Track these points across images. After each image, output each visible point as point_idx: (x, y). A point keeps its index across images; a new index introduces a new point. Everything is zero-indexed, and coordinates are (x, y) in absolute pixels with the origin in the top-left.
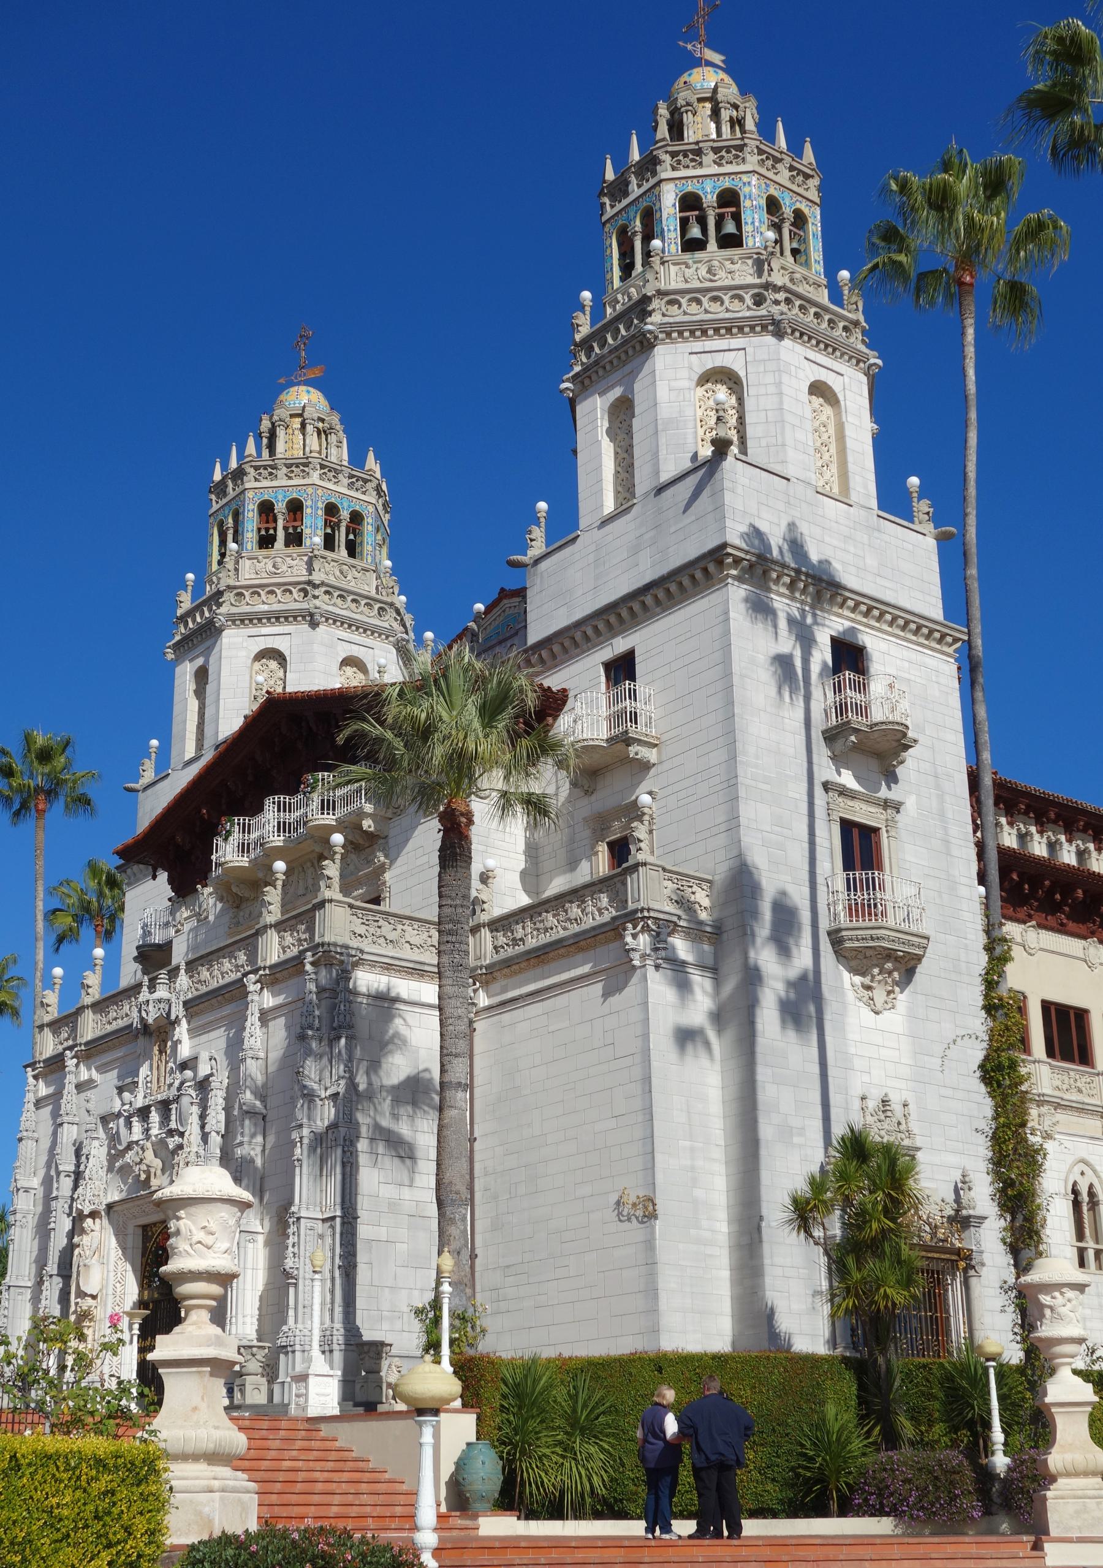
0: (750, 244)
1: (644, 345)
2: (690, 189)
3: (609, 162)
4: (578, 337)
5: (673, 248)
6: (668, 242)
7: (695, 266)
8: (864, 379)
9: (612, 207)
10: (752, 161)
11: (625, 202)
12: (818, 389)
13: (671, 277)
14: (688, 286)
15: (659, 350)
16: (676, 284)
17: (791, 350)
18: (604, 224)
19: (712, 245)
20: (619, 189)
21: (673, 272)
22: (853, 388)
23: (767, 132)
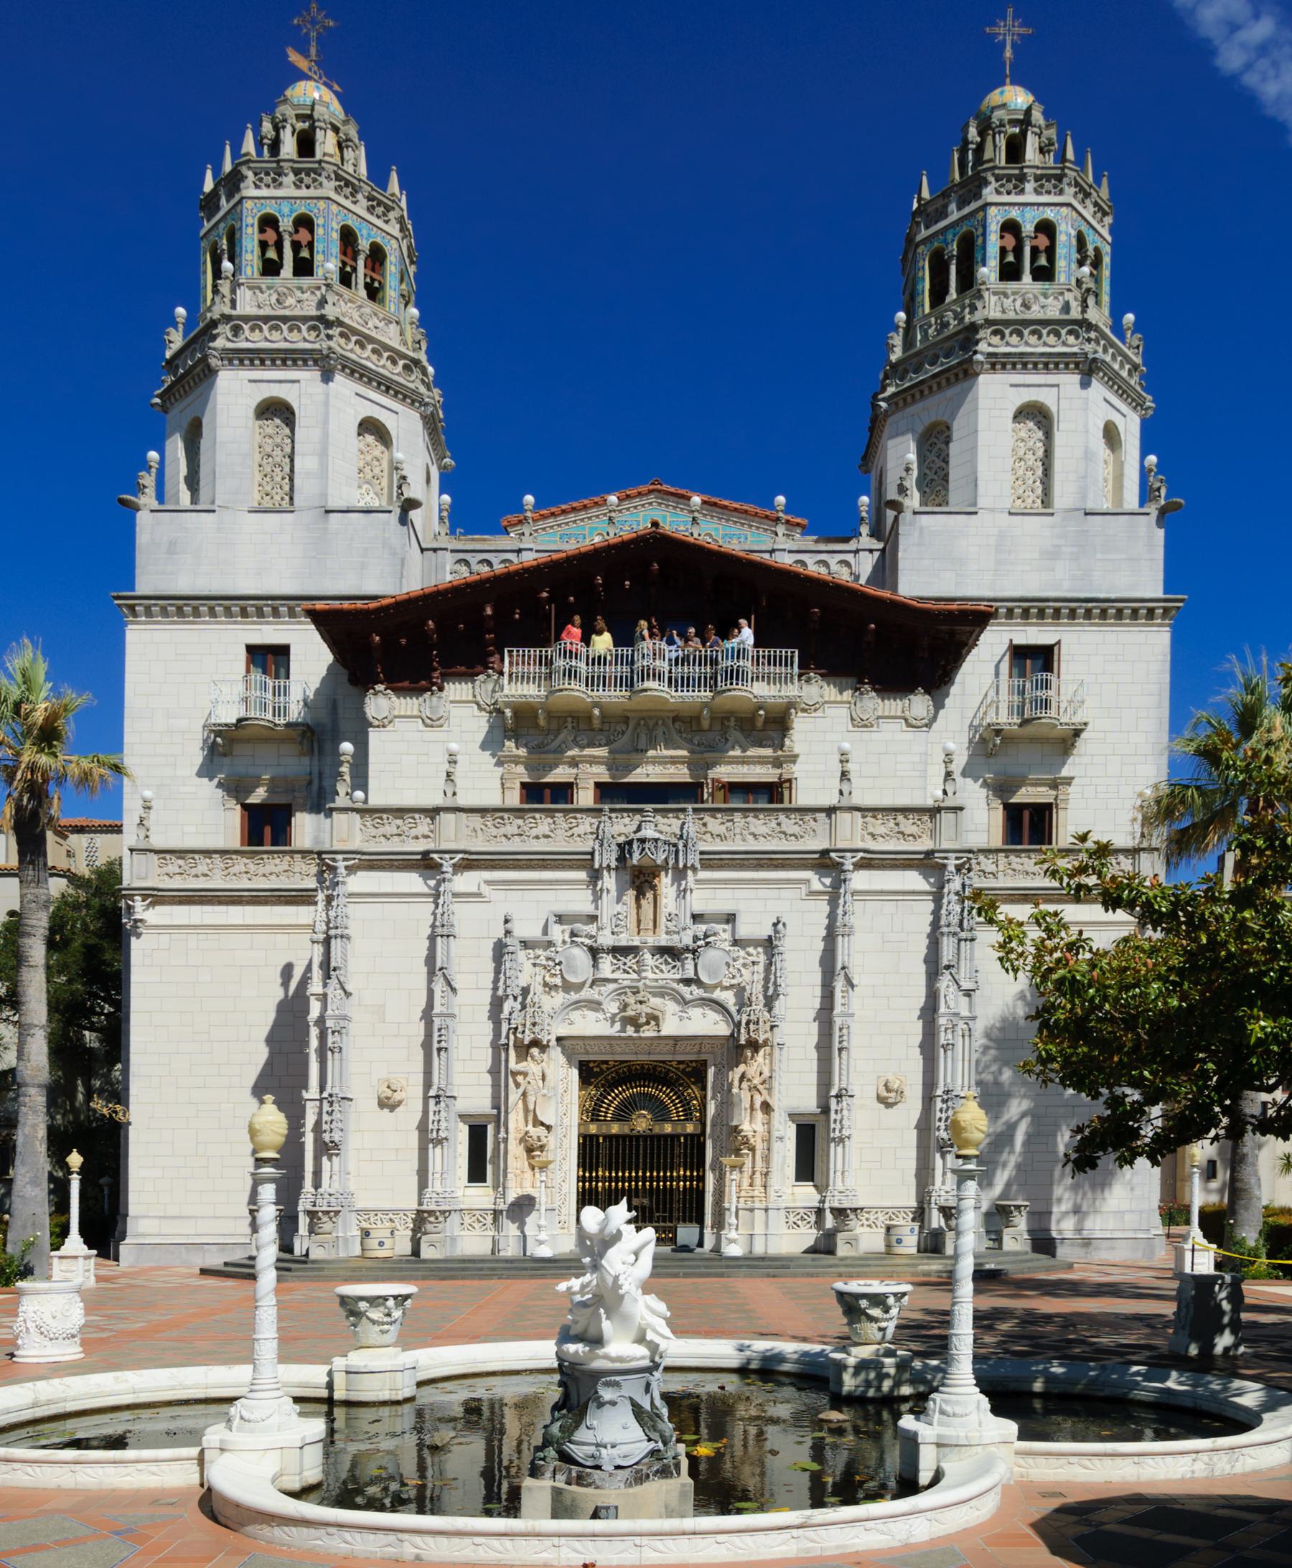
1: (965, 373)
6: (988, 272)
10: (1069, 195)
13: (991, 307)
14: (1005, 317)
16: (995, 314)
19: (1027, 277)
23: (1080, 161)
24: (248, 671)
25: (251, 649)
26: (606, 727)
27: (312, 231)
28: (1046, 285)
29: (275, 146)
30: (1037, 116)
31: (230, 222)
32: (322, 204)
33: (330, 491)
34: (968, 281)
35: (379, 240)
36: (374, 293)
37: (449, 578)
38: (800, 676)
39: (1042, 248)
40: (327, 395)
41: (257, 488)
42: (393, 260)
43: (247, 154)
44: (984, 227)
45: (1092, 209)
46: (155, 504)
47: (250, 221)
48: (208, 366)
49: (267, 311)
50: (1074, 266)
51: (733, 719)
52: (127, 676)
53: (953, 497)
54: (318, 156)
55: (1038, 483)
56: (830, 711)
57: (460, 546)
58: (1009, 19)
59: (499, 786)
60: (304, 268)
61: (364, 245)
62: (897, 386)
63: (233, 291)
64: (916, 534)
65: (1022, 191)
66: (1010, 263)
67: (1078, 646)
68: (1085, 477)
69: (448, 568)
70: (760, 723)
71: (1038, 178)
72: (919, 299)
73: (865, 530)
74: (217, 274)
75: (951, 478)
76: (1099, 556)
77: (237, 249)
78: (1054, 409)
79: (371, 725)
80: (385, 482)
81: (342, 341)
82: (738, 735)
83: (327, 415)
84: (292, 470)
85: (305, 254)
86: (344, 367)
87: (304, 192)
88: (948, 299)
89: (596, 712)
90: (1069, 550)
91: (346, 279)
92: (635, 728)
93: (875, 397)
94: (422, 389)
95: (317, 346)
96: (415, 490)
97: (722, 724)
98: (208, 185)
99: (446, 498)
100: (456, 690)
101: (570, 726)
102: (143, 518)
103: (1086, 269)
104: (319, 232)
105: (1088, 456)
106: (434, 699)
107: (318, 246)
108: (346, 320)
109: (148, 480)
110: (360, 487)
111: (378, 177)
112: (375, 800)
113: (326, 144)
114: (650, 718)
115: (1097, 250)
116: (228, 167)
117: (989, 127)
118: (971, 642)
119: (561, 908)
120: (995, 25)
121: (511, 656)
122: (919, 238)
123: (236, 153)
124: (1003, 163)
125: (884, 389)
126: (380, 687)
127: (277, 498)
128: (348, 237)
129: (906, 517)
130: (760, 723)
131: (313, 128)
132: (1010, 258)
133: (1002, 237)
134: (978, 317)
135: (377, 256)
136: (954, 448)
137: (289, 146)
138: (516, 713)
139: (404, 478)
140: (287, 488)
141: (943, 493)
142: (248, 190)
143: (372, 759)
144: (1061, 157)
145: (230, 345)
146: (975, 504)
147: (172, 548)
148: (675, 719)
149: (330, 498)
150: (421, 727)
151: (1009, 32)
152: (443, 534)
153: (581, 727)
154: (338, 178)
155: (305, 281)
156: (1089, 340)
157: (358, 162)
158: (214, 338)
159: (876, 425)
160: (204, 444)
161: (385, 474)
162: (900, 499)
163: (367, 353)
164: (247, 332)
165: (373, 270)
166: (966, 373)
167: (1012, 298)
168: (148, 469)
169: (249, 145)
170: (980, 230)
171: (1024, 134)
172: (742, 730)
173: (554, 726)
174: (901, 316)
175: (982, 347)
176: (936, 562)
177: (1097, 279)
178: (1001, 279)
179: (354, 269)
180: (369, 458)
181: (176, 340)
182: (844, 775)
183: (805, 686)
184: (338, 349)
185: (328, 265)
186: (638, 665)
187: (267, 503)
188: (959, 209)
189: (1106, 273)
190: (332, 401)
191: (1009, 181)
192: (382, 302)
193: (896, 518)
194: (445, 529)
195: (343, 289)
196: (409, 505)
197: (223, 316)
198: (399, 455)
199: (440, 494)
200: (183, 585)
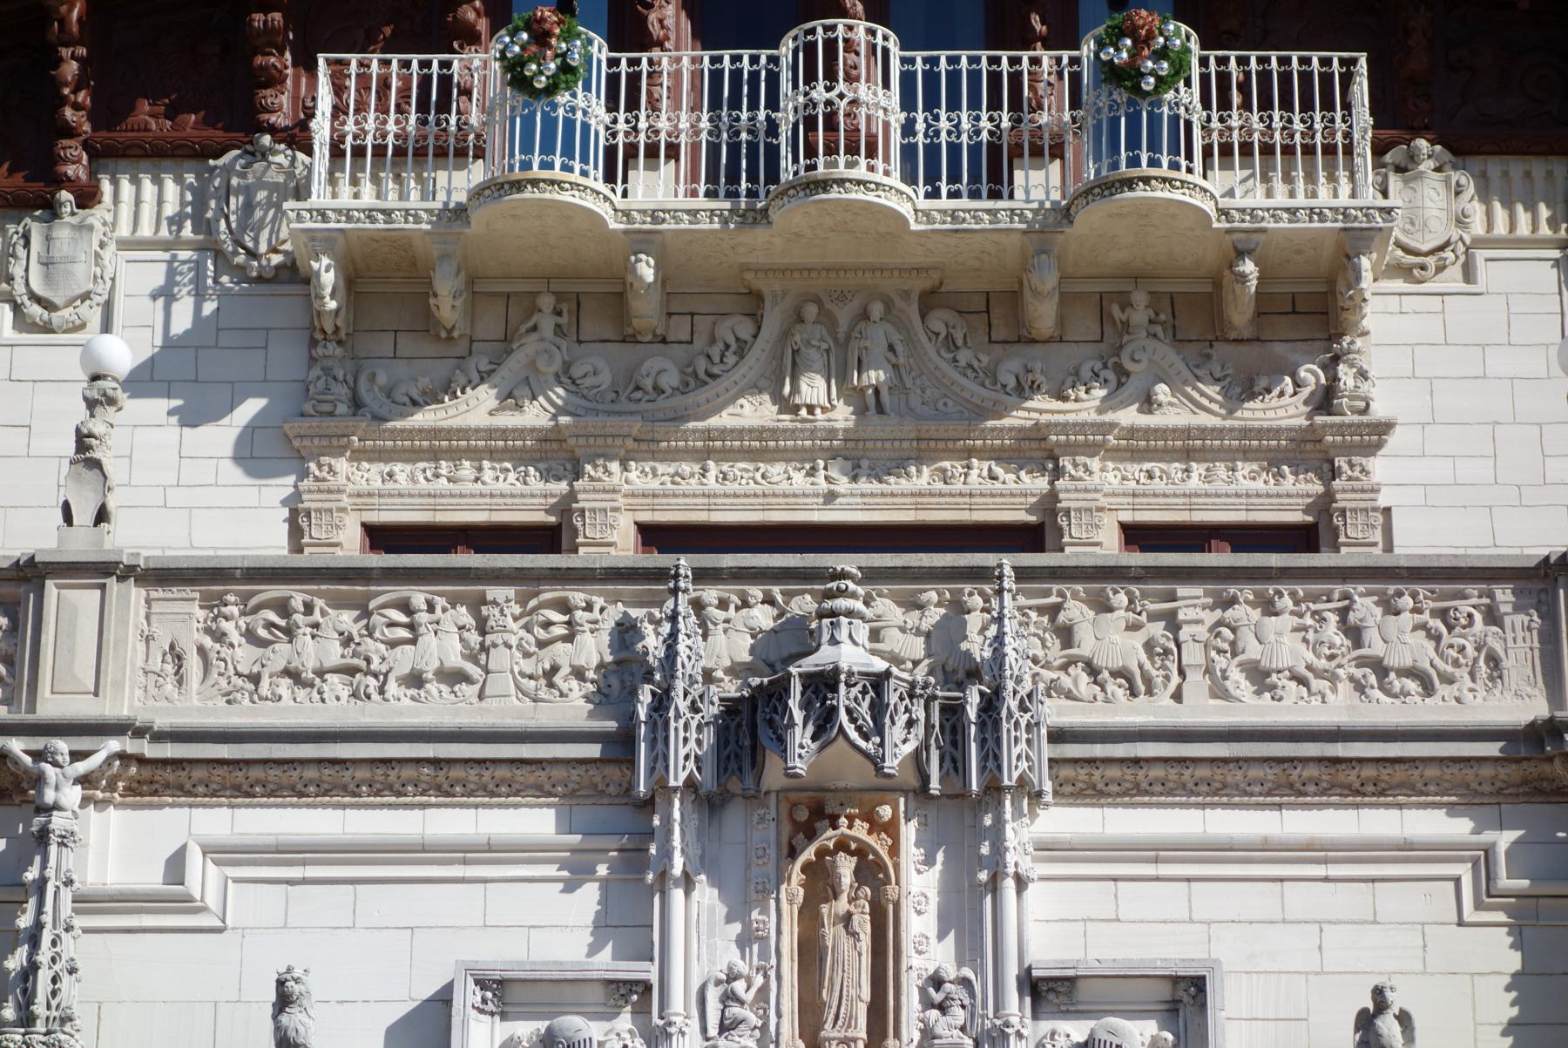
26: (680, 329)
38: (1379, 150)
51: (1140, 298)
70: (1240, 315)
82: (1165, 353)
89: (647, 270)
92: (786, 334)
97: (1103, 316)
101: (547, 323)
114: (842, 297)
119: (503, 952)
121: (339, 89)
130: (1240, 315)
138: (352, 282)
148: (930, 300)
150: (9, 333)
153: (589, 328)
172: (1178, 340)
173: (490, 324)
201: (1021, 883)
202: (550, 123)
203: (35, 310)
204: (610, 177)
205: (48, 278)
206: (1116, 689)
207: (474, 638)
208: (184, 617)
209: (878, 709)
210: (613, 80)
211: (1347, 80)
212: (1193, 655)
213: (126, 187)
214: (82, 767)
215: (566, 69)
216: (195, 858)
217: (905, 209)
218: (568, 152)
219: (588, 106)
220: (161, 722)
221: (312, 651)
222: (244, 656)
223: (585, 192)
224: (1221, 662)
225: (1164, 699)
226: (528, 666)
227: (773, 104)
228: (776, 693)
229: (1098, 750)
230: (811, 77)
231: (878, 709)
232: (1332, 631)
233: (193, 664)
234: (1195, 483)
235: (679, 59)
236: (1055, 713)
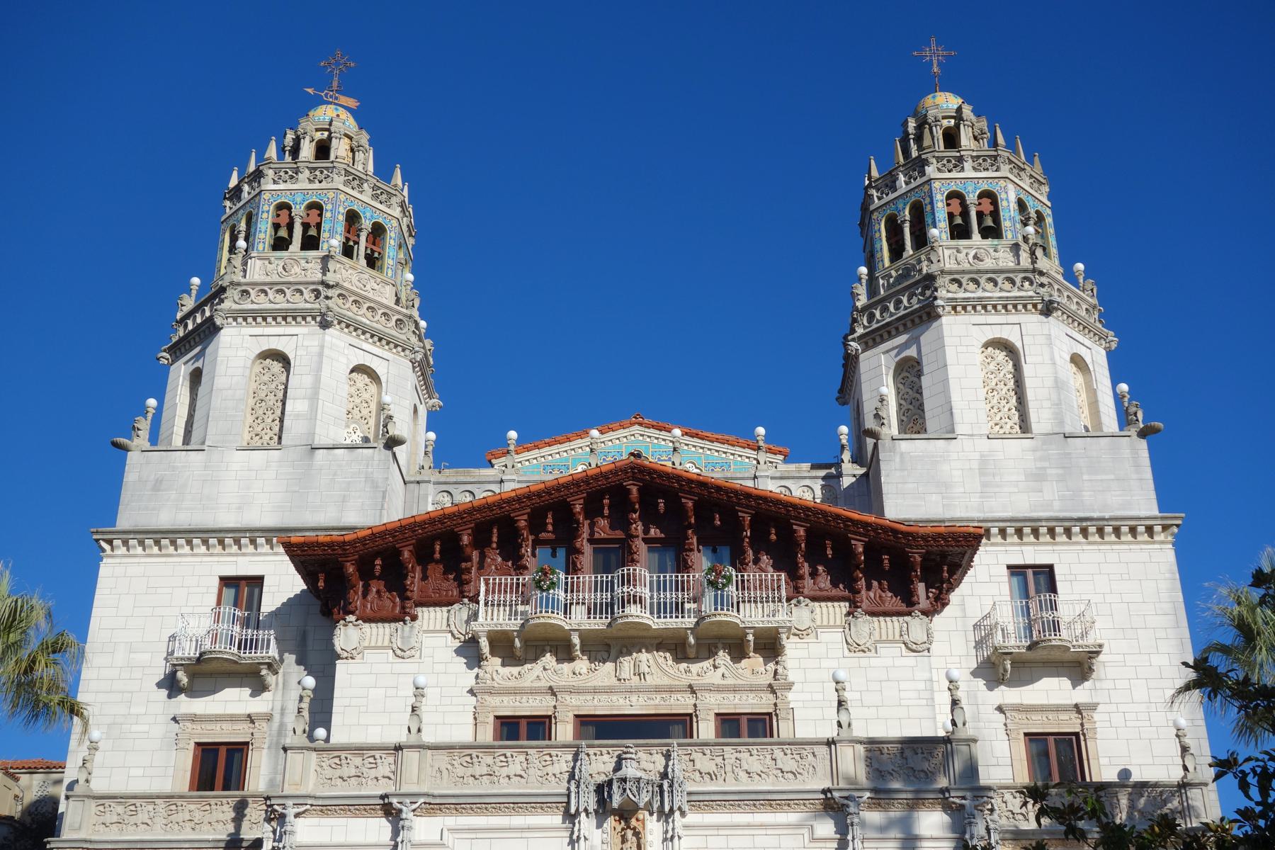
0: (1010, 236)
1: (927, 315)
2: (954, 188)
3: (873, 162)
4: (859, 304)
5: (944, 236)
6: (938, 232)
7: (965, 251)
8: (1104, 353)
9: (879, 199)
10: (1005, 170)
11: (892, 196)
12: (1077, 360)
15: (944, 319)
16: (950, 265)
17: (1055, 326)
18: (872, 212)
19: (976, 236)
20: (889, 183)
21: (948, 254)
22: (1097, 357)
24: (219, 603)
25: (226, 581)
27: (320, 215)
28: (996, 242)
29: (295, 151)
30: (967, 111)
31: (248, 209)
32: (331, 194)
33: (317, 431)
34: (921, 240)
35: (380, 220)
36: (372, 262)
37: (430, 508)
38: (788, 600)
39: (987, 212)
40: (322, 347)
41: (247, 429)
42: (393, 235)
43: (269, 158)
44: (931, 198)
45: (1028, 181)
46: (147, 446)
47: (266, 208)
48: (214, 324)
49: (276, 278)
50: (1019, 226)
52: (96, 612)
53: (930, 424)
54: (332, 157)
55: (1013, 411)
56: (825, 636)
57: (443, 479)
58: (934, 46)
59: (472, 721)
60: (310, 243)
61: (367, 224)
62: (865, 327)
63: (245, 264)
64: (898, 459)
65: (963, 169)
66: (959, 225)
67: (1073, 562)
68: (1059, 404)
69: (430, 500)
71: (975, 158)
72: (878, 255)
73: (846, 456)
74: (233, 249)
75: (926, 407)
76: (1085, 477)
77: (252, 230)
78: (1018, 345)
79: (339, 657)
80: (372, 422)
81: (340, 301)
83: (320, 363)
84: (283, 413)
85: (313, 232)
86: (340, 323)
87: (317, 185)
88: (905, 255)
90: (1054, 471)
91: (348, 251)
93: (845, 338)
94: (414, 340)
95: (317, 306)
96: (400, 428)
98: (234, 182)
99: (432, 436)
100: (430, 617)
102: (133, 457)
103: (1030, 229)
104: (327, 215)
105: (1059, 385)
106: (407, 628)
107: (325, 226)
108: (346, 284)
109: (144, 425)
110: (348, 426)
111: (383, 172)
112: (338, 737)
113: (340, 149)
115: (1038, 212)
116: (252, 168)
117: (925, 122)
118: (964, 562)
120: (922, 50)
121: (487, 584)
122: (872, 208)
123: (260, 158)
124: (942, 148)
125: (853, 331)
126: (351, 618)
127: (267, 437)
128: (352, 218)
129: (884, 444)
131: (330, 138)
132: (959, 220)
133: (948, 205)
134: (934, 269)
135: (378, 231)
136: (926, 381)
137: (307, 151)
139: (391, 417)
140: (276, 429)
141: (920, 421)
142: (267, 184)
143: (337, 693)
144: (994, 143)
145: (235, 307)
146: (953, 431)
147: (158, 485)
149: (317, 438)
151: (934, 55)
152: (426, 467)
154: (347, 173)
155: (312, 254)
156: (1042, 285)
157: (366, 162)
158: (222, 301)
159: (850, 363)
160: (202, 390)
161: (374, 414)
162: (877, 428)
163: (364, 310)
164: (253, 296)
165: (374, 244)
166: (929, 314)
167: (965, 251)
168: (145, 415)
169: (272, 152)
170: (928, 200)
171: (957, 126)
174: (863, 270)
175: (942, 293)
176: (918, 488)
177: (1043, 236)
178: (952, 238)
179: (357, 243)
180: (358, 401)
181: (189, 303)
182: (841, 704)
183: (794, 610)
184: (336, 308)
185: (333, 241)
186: (618, 590)
187: (257, 442)
188: (907, 184)
189: (1051, 231)
190: (326, 352)
191: (949, 161)
192: (381, 269)
193: (876, 445)
194: (428, 462)
195: (345, 260)
196: (392, 443)
197: (232, 283)
198: (387, 399)
199: (428, 430)
200: (164, 519)
201: (679, 838)
202: (547, 598)
203: (399, 652)
204: (565, 613)
205: (403, 643)
206: (707, 778)
207: (525, 765)
208: (442, 759)
209: (638, 789)
210: (566, 583)
211: (779, 580)
212: (728, 768)
213: (426, 614)
214: (414, 806)
215: (553, 583)
216: (445, 833)
217: (650, 623)
218: (553, 607)
219: (560, 594)
220: (436, 792)
221: (479, 770)
222: (460, 771)
223: (558, 619)
224: (736, 770)
225: (721, 780)
226: (540, 773)
227: (613, 590)
228: (610, 783)
229: (701, 798)
230: (623, 584)
231: (638, 789)
232: (768, 761)
233: (445, 772)
234: (737, 701)
235: (587, 578)
236: (690, 787)
